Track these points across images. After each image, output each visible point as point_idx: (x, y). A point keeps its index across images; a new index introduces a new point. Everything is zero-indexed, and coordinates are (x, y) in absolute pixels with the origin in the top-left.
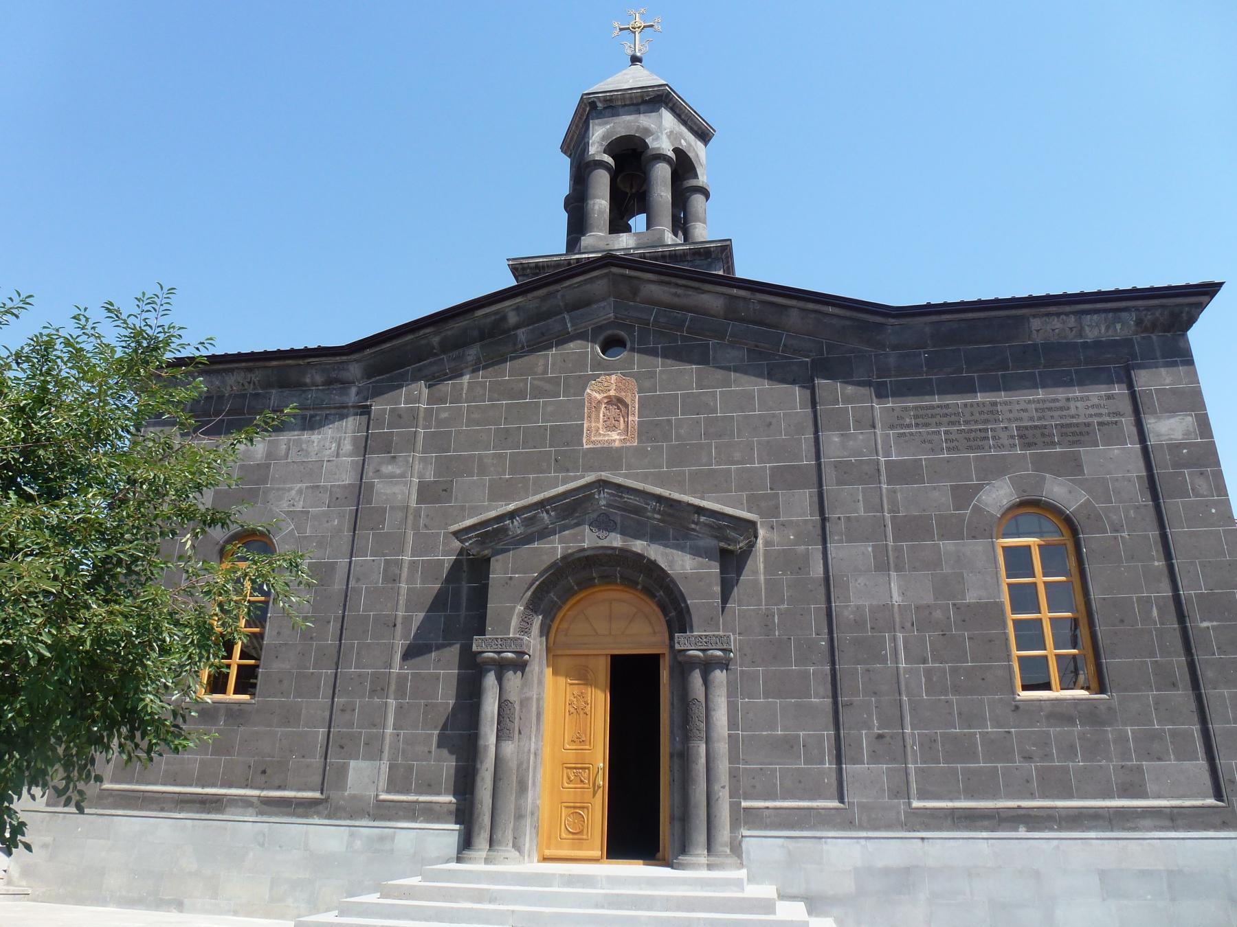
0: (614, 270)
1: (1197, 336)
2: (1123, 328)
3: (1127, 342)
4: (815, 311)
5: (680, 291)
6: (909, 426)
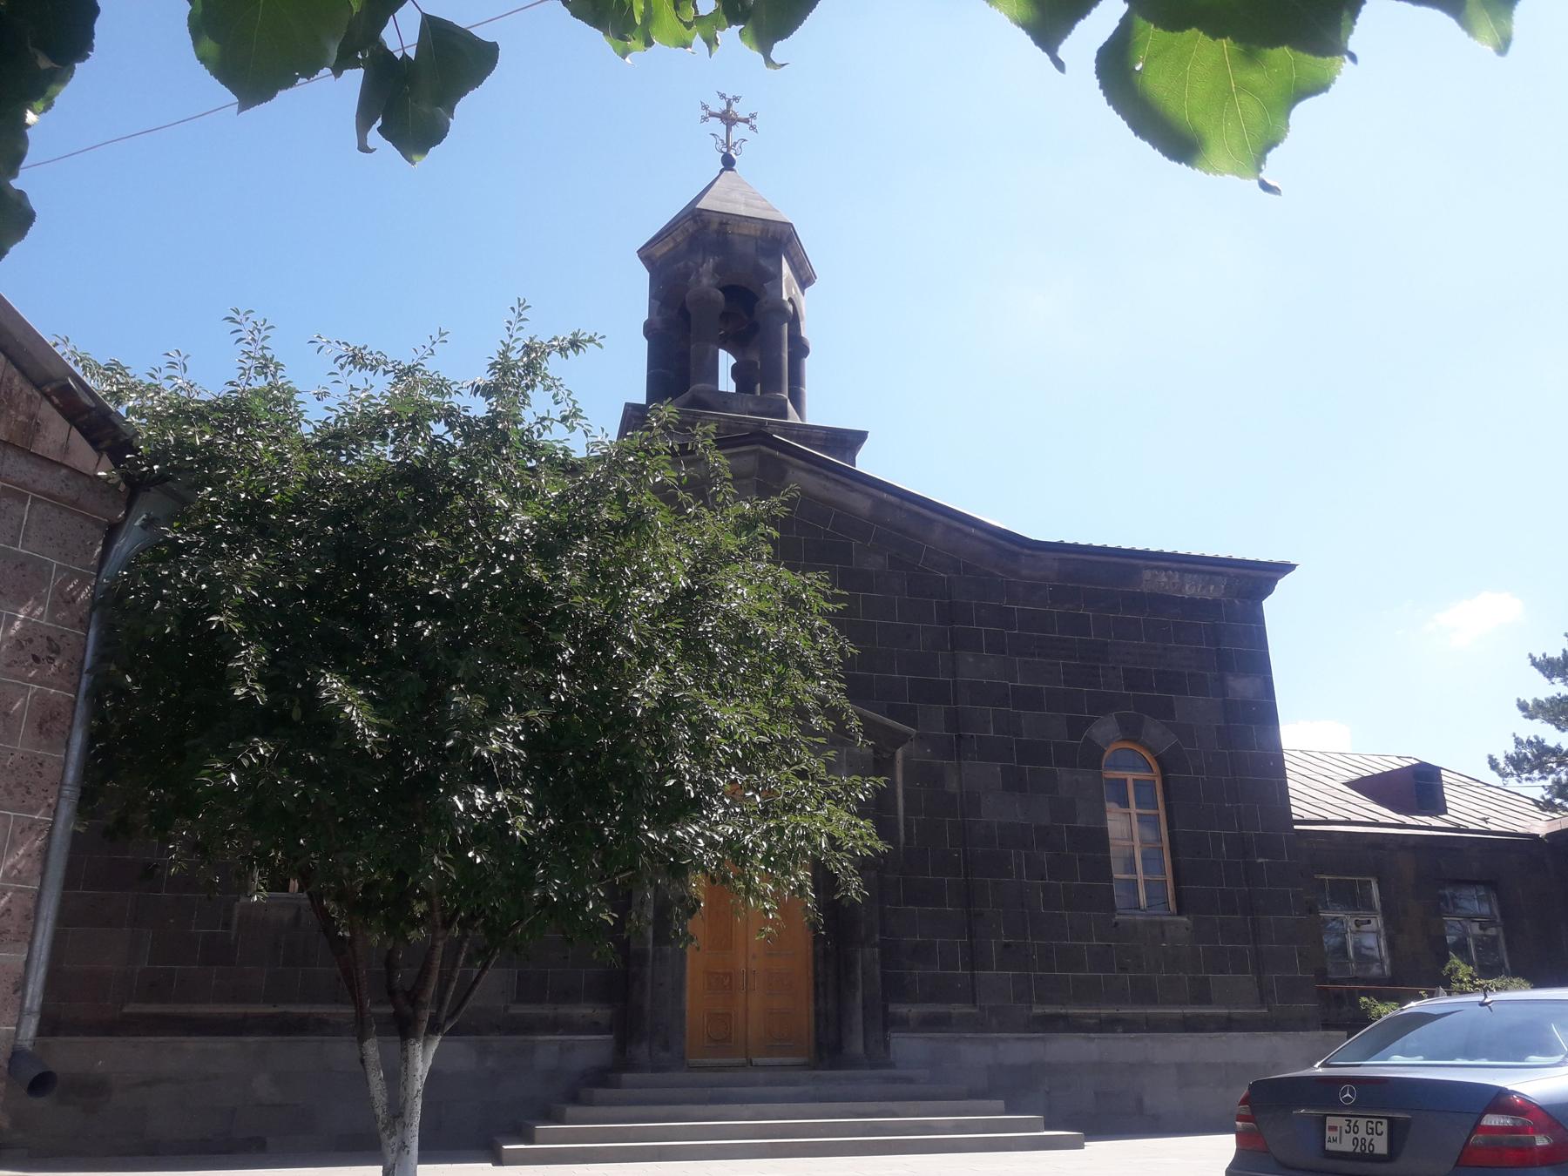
0: (764, 448)
1: (1269, 605)
2: (1212, 592)
3: (1216, 604)
4: (958, 530)
5: (828, 484)
6: (1033, 655)
